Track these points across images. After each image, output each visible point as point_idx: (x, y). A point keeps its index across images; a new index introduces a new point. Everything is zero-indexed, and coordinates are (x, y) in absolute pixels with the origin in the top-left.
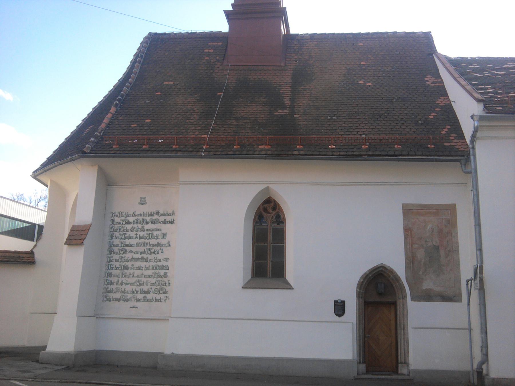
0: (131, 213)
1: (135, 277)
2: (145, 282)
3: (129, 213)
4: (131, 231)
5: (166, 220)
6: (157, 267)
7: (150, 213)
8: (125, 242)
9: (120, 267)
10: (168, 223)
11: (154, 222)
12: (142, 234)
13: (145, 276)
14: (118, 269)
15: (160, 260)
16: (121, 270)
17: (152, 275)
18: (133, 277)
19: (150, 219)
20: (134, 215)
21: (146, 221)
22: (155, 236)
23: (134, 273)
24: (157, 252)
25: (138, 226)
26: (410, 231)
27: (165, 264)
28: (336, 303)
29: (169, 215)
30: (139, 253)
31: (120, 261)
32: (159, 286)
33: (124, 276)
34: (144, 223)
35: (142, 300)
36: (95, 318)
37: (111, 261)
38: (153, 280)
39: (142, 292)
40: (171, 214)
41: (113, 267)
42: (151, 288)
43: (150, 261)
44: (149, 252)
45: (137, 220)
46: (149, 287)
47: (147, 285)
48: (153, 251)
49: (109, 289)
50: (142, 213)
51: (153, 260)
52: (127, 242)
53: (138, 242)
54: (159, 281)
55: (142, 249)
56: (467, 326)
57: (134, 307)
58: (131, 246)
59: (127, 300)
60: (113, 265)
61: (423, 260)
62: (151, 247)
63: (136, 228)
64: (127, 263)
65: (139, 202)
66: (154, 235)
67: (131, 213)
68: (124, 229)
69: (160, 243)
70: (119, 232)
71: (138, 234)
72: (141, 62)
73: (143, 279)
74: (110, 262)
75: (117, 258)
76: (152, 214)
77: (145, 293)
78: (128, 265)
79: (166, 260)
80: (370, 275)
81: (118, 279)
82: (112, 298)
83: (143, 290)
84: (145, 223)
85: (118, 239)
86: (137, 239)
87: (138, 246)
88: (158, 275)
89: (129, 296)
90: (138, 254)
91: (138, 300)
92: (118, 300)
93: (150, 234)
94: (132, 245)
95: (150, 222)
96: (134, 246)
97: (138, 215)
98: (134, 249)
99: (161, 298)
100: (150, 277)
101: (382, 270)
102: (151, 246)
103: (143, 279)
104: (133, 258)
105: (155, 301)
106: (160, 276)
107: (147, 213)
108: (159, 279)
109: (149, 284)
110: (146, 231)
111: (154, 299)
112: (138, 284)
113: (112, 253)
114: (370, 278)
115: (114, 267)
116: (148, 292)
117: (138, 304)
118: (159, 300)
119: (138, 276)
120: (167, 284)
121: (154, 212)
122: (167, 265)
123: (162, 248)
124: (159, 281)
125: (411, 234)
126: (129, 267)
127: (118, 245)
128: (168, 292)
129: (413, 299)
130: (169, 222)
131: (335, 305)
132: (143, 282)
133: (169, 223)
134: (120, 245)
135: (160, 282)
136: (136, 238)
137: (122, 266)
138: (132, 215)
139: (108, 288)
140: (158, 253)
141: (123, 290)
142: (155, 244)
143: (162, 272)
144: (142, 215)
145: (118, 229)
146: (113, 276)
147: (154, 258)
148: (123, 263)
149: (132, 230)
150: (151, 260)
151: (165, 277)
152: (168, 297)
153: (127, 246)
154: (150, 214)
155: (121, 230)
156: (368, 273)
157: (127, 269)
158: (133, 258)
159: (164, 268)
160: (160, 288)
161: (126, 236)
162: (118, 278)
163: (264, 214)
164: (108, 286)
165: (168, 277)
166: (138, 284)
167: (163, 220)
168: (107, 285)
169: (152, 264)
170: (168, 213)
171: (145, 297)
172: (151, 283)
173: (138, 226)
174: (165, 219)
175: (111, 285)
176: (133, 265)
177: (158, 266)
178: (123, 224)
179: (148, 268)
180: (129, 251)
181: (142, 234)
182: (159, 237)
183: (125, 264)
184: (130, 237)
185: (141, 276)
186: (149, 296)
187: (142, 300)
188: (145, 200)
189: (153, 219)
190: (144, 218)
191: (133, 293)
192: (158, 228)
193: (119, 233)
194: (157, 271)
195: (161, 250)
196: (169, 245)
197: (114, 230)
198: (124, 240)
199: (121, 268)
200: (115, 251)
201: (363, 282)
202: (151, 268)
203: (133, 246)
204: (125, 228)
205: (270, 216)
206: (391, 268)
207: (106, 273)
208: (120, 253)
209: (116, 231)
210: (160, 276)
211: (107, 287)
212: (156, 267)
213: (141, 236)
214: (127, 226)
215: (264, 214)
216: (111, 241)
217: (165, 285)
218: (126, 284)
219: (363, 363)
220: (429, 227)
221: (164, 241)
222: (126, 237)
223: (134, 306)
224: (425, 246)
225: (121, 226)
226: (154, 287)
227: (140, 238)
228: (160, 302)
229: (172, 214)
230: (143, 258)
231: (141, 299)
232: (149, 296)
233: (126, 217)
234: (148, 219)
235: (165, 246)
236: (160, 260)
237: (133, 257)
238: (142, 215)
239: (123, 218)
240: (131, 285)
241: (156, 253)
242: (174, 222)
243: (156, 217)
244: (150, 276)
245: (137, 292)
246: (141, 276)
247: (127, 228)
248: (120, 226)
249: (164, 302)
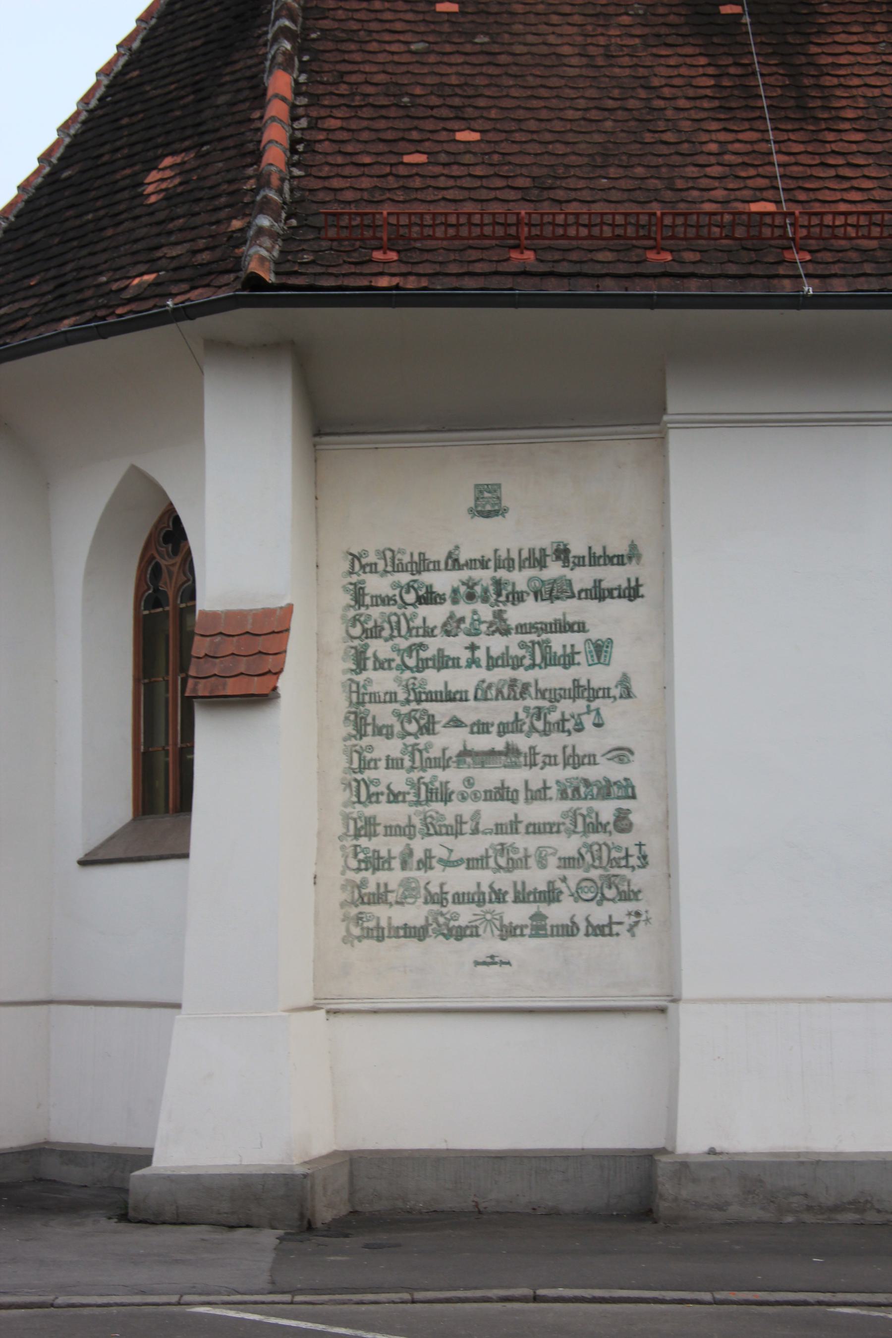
0: (438, 553)
1: (484, 833)
2: (532, 851)
4: (448, 633)
5: (604, 585)
6: (582, 790)
7: (525, 554)
9: (412, 791)
10: (612, 598)
12: (497, 644)
13: (531, 829)
14: (404, 801)
15: (591, 759)
16: (418, 803)
17: (562, 820)
18: (475, 831)
19: (530, 579)
20: (453, 562)
21: (510, 588)
22: (560, 652)
23: (477, 814)
24: (573, 722)
25: (475, 612)
27: (616, 772)
29: (615, 560)
30: (494, 729)
31: (407, 763)
32: (596, 867)
33: (432, 828)
34: (503, 599)
35: (527, 931)
36: (322, 1013)
37: (364, 765)
38: (569, 845)
39: (521, 897)
40: (622, 556)
41: (378, 794)
42: (564, 880)
43: (547, 760)
44: (540, 725)
45: (470, 584)
46: (552, 872)
47: (542, 864)
48: (554, 717)
49: (372, 888)
50: (489, 554)
51: (560, 759)
52: (434, 680)
53: (483, 681)
54: (596, 847)
57: (491, 961)
58: (450, 697)
59: (460, 934)
60: (377, 782)
62: (545, 704)
63: (468, 621)
64: (442, 775)
65: (472, 504)
66: (553, 650)
67: (438, 553)
68: (412, 624)
69: (583, 682)
70: (392, 637)
71: (478, 648)
73: (523, 842)
74: (361, 770)
75: (396, 754)
76: (537, 560)
77: (535, 901)
78: (447, 782)
79: (619, 756)
81: (408, 845)
82: (390, 924)
83: (529, 888)
84: (507, 597)
85: (390, 668)
86: (479, 666)
87: (486, 699)
88: (588, 820)
89: (466, 914)
90: (488, 732)
91: (509, 932)
92: (419, 933)
93: (537, 646)
94: (458, 696)
95: (528, 594)
96: (466, 700)
97: (471, 564)
98: (469, 712)
99: (614, 919)
100: (555, 829)
102: (543, 698)
103: (523, 842)
104: (465, 753)
105: (587, 935)
106: (598, 827)
107: (514, 555)
108: (593, 838)
109: (553, 861)
110: (517, 633)
111: (583, 926)
112: (502, 862)
113: (369, 729)
115: (382, 794)
116: (551, 895)
118: (603, 926)
119: (499, 829)
120: (633, 861)
121: (543, 550)
122: (626, 779)
123: (594, 705)
124: (596, 847)
126: (453, 792)
127: (392, 697)
128: (640, 891)
130: (616, 593)
132: (521, 854)
133: (619, 597)
134: (401, 696)
135: (600, 849)
136: (473, 662)
137: (419, 789)
138: (442, 566)
139: (364, 883)
140: (580, 728)
141: (434, 889)
142: (561, 689)
143: (606, 810)
144: (491, 564)
145: (386, 626)
146: (380, 829)
147: (565, 748)
148: (422, 774)
149: (449, 628)
150: (550, 760)
151: (622, 831)
152: (643, 911)
153: (433, 697)
154: (529, 559)
155: (399, 630)
157: (446, 798)
158: (465, 753)
159: (615, 789)
160: (601, 876)
161: (423, 655)
162: (404, 840)
164: (364, 874)
165: (634, 829)
166: (502, 862)
167: (589, 585)
168: (359, 870)
169: (555, 774)
170: (610, 552)
171: (538, 917)
172: (558, 855)
173: (475, 612)
174: (600, 581)
175: (376, 869)
176: (469, 782)
177: (587, 783)
178: (405, 604)
179: (540, 795)
180: (445, 721)
181: (497, 644)
182: (577, 658)
183: (435, 777)
184: (443, 662)
185: (513, 826)
186: (557, 913)
187: (527, 931)
188: (499, 498)
189: (544, 579)
190: (502, 574)
191: (481, 903)
192: (570, 619)
193: (390, 643)
194: (583, 806)
195: (593, 714)
196: (628, 694)
197: (364, 631)
198: (418, 671)
199: (418, 795)
200: (379, 722)
202: (553, 792)
203: (461, 700)
204: (418, 622)
207: (347, 818)
208: (403, 728)
209: (374, 633)
210: (598, 827)
211: (358, 877)
212: (577, 789)
213: (496, 652)
214: (424, 610)
216: (361, 678)
217: (623, 863)
218: (447, 863)
222: (427, 659)
223: (492, 957)
225: (399, 612)
226: (574, 875)
227: (493, 662)
228: (611, 935)
229: (630, 558)
230: (511, 751)
231: (522, 927)
232: (557, 913)
233: (419, 572)
234: (520, 579)
235: (609, 697)
236: (591, 759)
237: (469, 748)
238: (491, 564)
239: (405, 578)
240: (468, 868)
241: (569, 725)
242: (642, 591)
243: (554, 570)
244: (551, 825)
245: (499, 897)
246: (513, 826)
247: (424, 620)
248: (395, 614)
249: (628, 934)
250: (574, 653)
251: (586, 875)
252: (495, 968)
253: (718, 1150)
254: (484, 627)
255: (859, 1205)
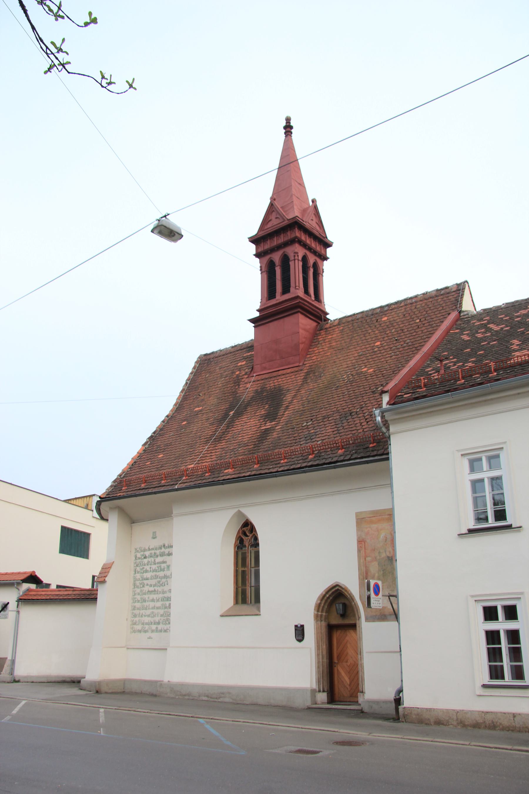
2: (157, 613)
3: (146, 548)
4: (147, 565)
5: (170, 552)
8: (144, 576)
11: (162, 555)
12: (154, 567)
16: (141, 603)
18: (149, 609)
20: (149, 549)
25: (151, 560)
26: (363, 543)
28: (296, 628)
30: (153, 586)
36: (126, 648)
37: (135, 594)
47: (158, 616)
48: (161, 583)
52: (145, 575)
55: (153, 582)
56: (399, 650)
57: (150, 638)
58: (147, 579)
59: (146, 631)
61: (377, 575)
62: (160, 580)
72: (185, 390)
73: (156, 611)
74: (134, 596)
80: (328, 596)
89: (147, 627)
91: (153, 631)
92: (140, 631)
101: (338, 589)
104: (149, 591)
108: (166, 610)
109: (159, 615)
114: (328, 598)
116: (159, 623)
117: (154, 635)
123: (167, 580)
125: (365, 545)
129: (367, 620)
131: (296, 630)
141: (143, 622)
156: (324, 593)
158: (149, 591)
162: (139, 611)
163: (244, 537)
167: (167, 553)
169: (161, 596)
177: (165, 597)
182: (165, 569)
184: (146, 571)
187: (155, 631)
190: (156, 551)
191: (149, 625)
194: (164, 602)
200: (137, 585)
201: (320, 604)
202: (160, 600)
204: (144, 563)
205: (248, 539)
206: (346, 587)
207: (132, 606)
211: (132, 619)
212: (163, 599)
215: (244, 537)
216: (135, 575)
218: (145, 616)
219: (324, 691)
220: (382, 536)
221: (168, 573)
224: (378, 557)
230: (155, 591)
231: (155, 630)
233: (144, 552)
239: (142, 553)
240: (148, 617)
241: (163, 585)
244: (159, 607)
250: (165, 568)
251: (164, 618)
252: (150, 639)
253: (170, 681)
254: (152, 563)
255: (189, 695)
